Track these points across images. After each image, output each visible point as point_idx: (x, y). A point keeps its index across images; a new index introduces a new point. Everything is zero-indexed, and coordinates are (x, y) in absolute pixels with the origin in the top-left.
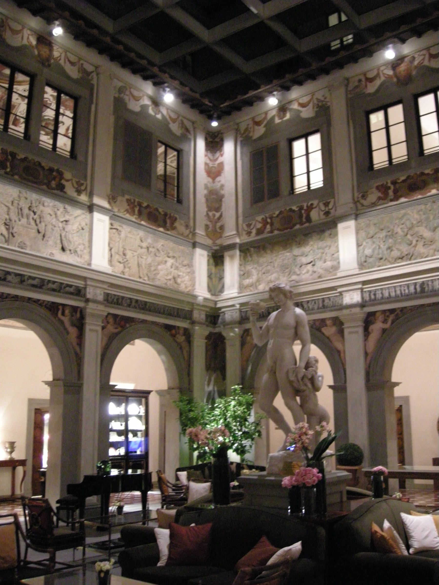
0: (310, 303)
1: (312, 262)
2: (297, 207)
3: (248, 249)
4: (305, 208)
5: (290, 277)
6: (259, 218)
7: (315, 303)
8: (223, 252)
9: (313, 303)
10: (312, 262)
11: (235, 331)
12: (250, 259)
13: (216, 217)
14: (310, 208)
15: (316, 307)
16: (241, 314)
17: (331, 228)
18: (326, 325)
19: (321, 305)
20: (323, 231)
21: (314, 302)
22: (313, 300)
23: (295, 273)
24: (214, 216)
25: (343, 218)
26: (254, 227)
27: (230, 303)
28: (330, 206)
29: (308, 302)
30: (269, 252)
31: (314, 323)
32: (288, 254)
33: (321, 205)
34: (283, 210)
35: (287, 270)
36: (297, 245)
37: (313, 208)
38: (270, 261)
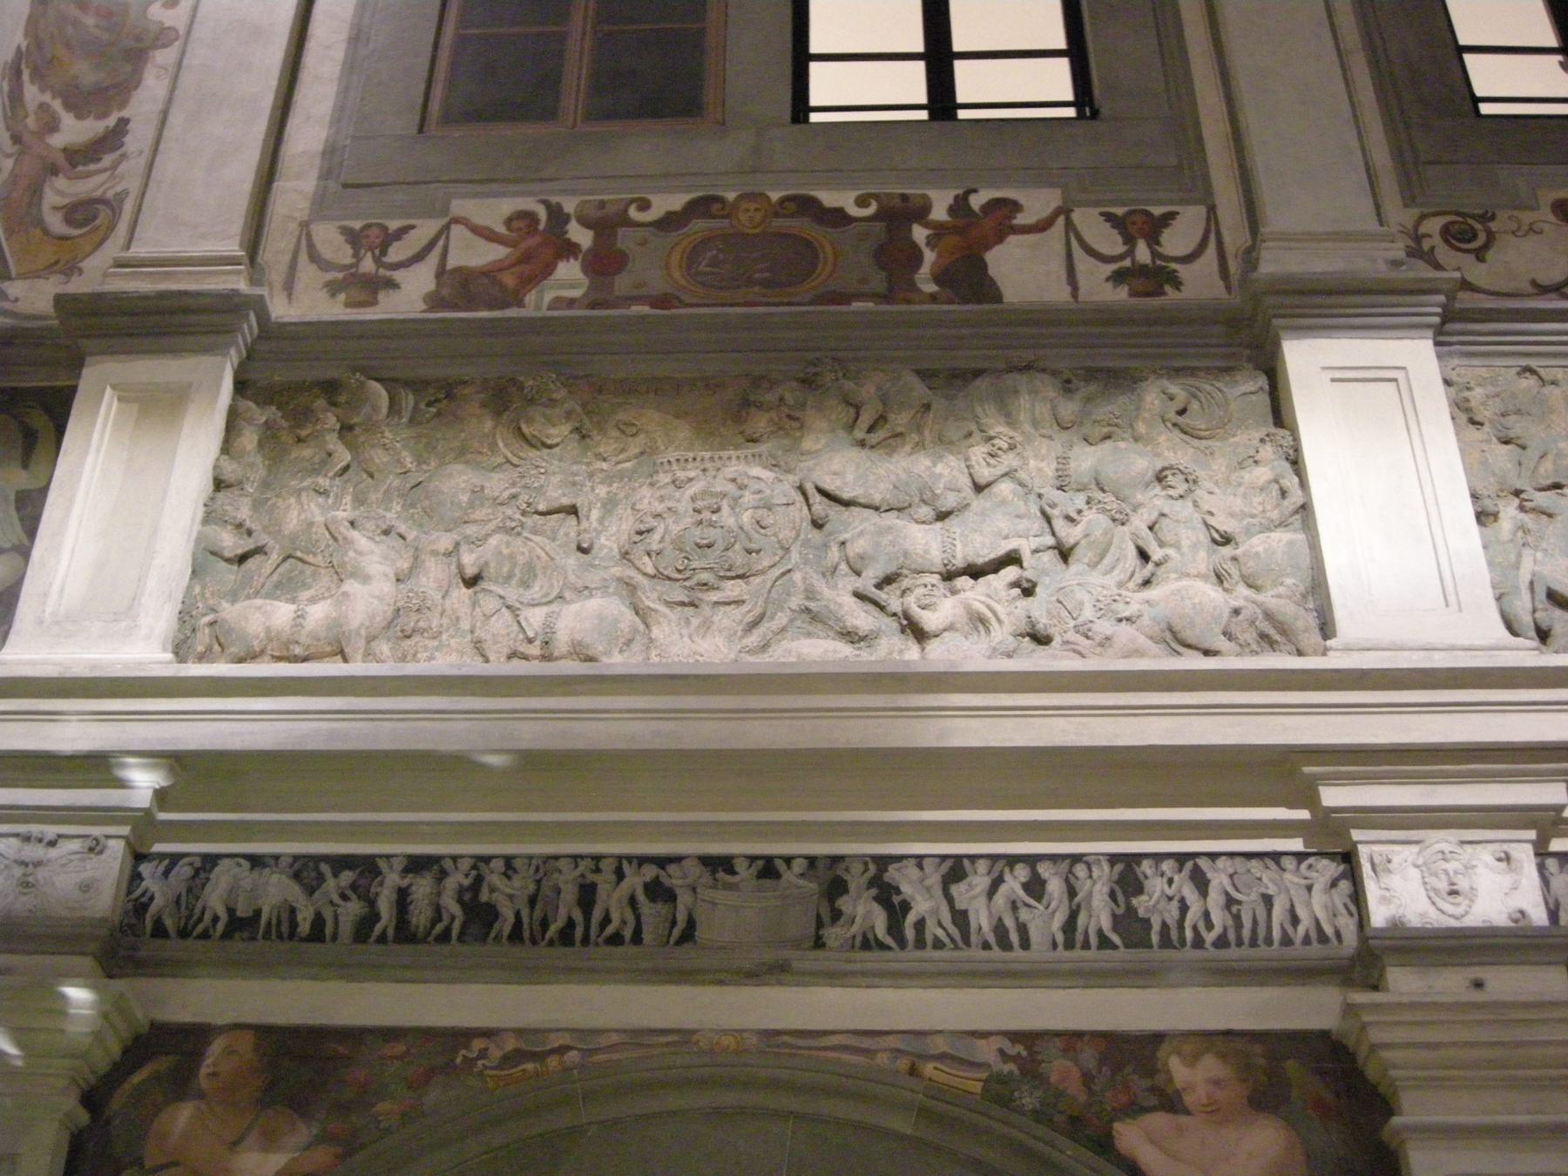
0: (979, 880)
1: (1012, 559)
2: (862, 202)
3: (330, 388)
4: (939, 213)
5: (764, 647)
6: (495, 211)
7: (1035, 887)
8: (76, 364)
9: (1014, 884)
10: (1012, 559)
11: (60, 1006)
12: (344, 456)
13: (58, 141)
14: (979, 229)
15: (1045, 921)
16: (136, 877)
17: (1192, 372)
18: (1171, 1103)
19: (1099, 914)
20: (1118, 380)
21: (1022, 873)
22: (1012, 860)
23: (815, 618)
24: (52, 126)
25: (1339, 303)
26: (419, 257)
27: (71, 733)
28: (1176, 241)
29: (956, 870)
30: (558, 432)
31: (1031, 1070)
32: (756, 471)
33: (1089, 222)
34: (731, 196)
35: (732, 589)
36: (833, 430)
37: (1004, 230)
38: (557, 495)
